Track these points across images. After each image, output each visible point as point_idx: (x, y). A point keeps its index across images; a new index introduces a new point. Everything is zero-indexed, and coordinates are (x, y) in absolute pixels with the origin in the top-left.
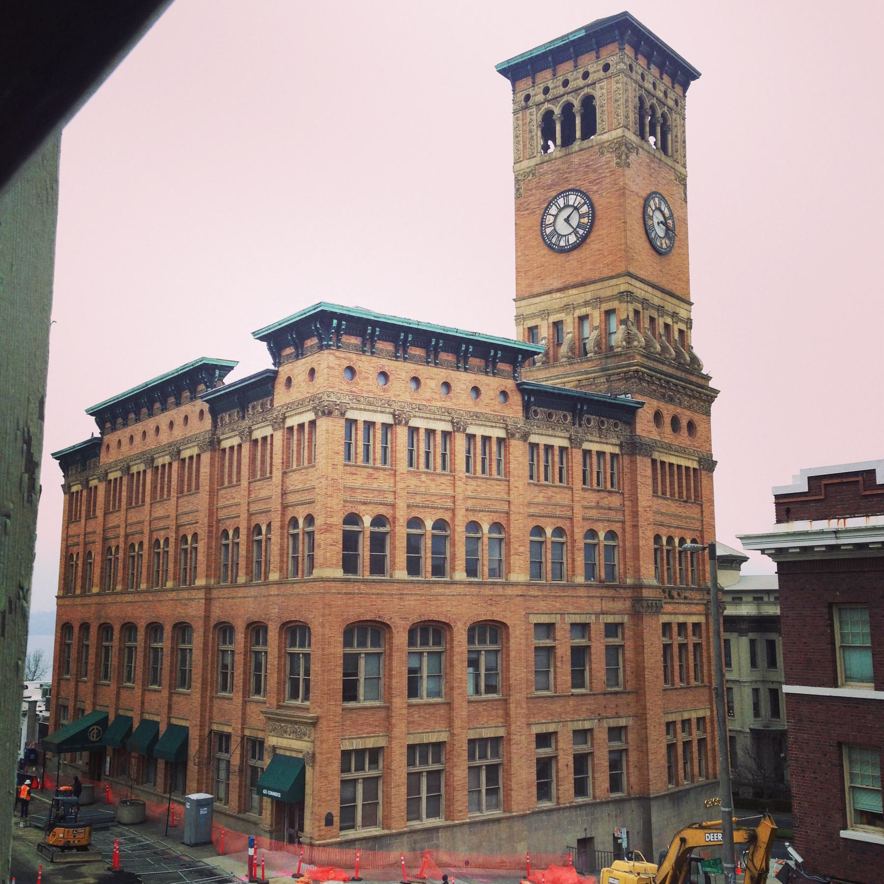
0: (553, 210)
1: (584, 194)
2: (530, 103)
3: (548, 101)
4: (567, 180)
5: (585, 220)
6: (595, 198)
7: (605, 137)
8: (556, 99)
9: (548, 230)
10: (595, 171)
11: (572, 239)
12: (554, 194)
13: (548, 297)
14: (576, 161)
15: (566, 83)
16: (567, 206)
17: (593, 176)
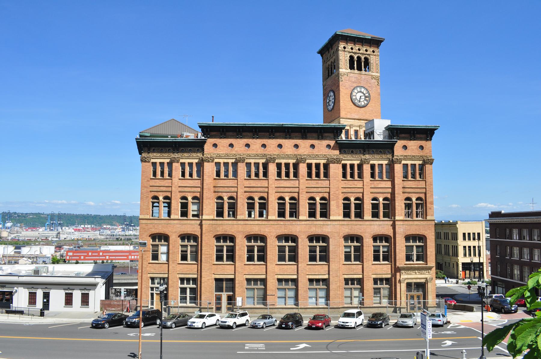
0: (356, 91)
1: (367, 90)
2: (346, 50)
3: (353, 53)
4: (360, 83)
5: (367, 99)
6: (370, 92)
7: (374, 74)
8: (355, 53)
9: (354, 97)
10: (370, 83)
11: (363, 104)
12: (355, 85)
14: (363, 77)
15: (359, 50)
16: (361, 92)
17: (369, 85)
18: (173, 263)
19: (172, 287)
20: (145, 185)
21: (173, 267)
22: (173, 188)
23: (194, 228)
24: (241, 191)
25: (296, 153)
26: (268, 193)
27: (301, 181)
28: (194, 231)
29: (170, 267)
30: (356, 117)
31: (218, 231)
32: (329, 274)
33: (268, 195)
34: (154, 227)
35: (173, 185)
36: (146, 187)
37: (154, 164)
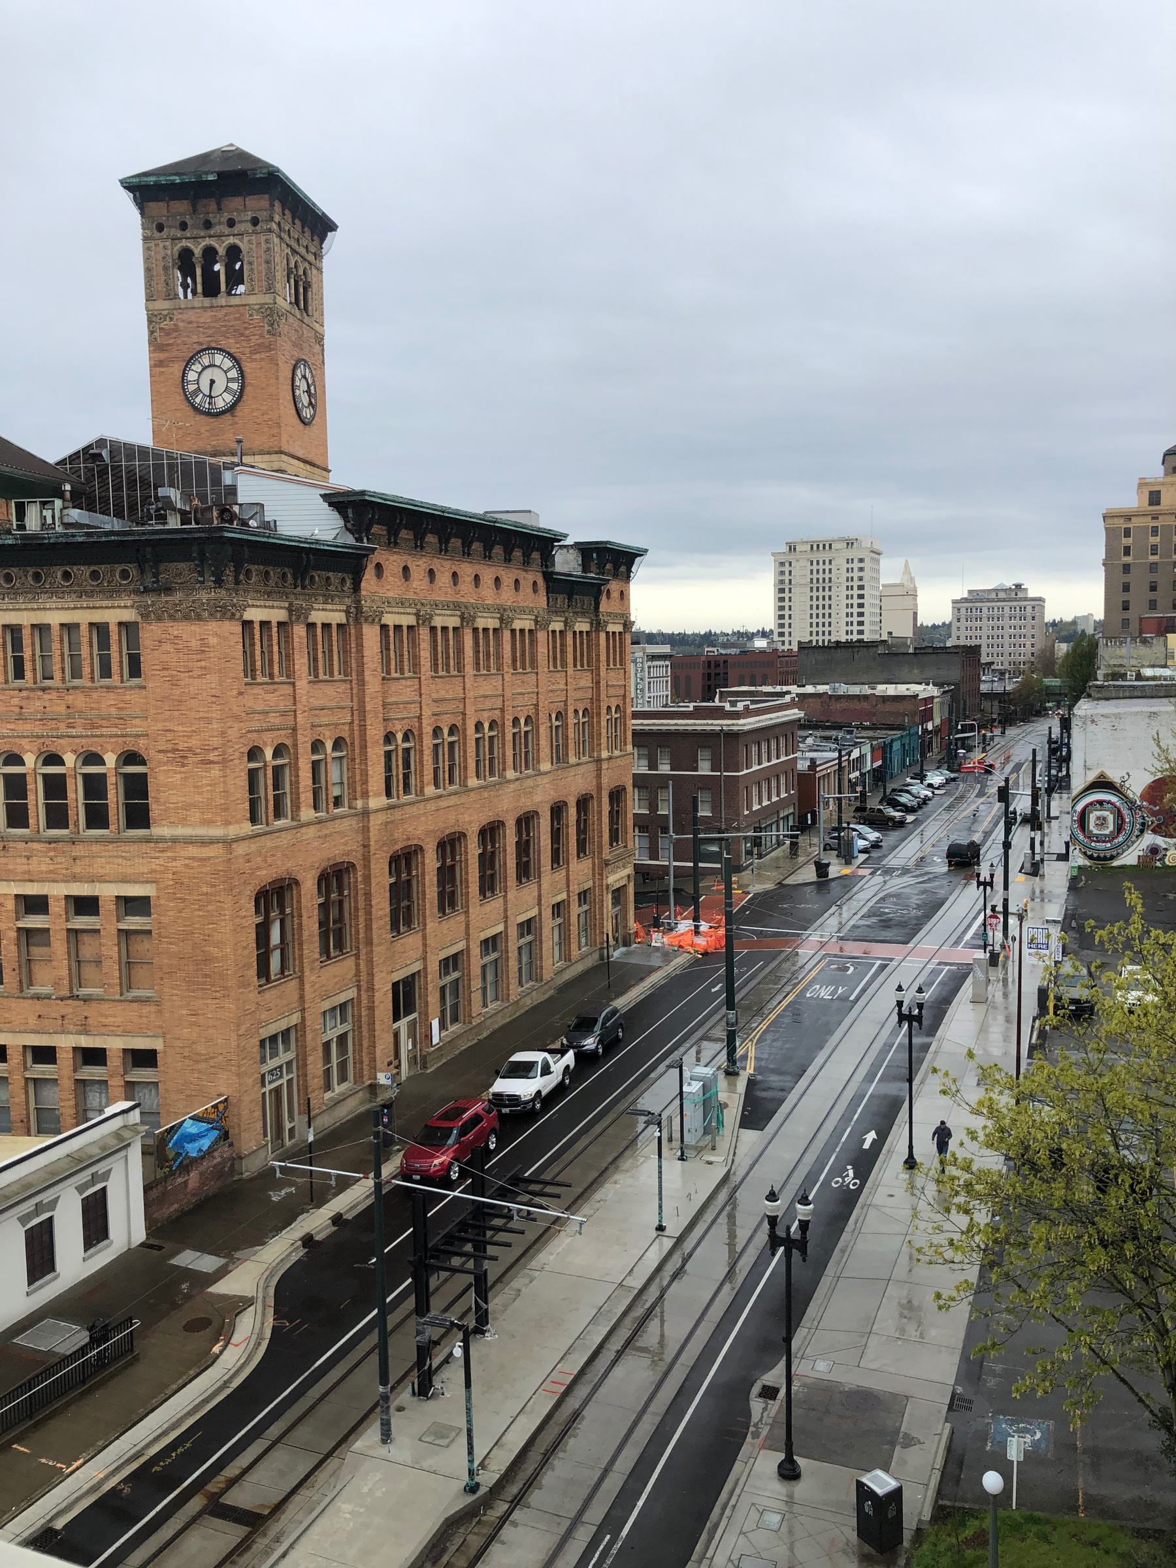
13: (302, 465)
18: (312, 969)
19: (314, 1049)
20: (237, 710)
21: (313, 984)
22: (300, 718)
23: (346, 844)
24: (427, 712)
25: (498, 601)
26: (464, 714)
27: (507, 677)
28: (348, 854)
29: (307, 986)
30: (300, 454)
31: (395, 842)
32: (539, 904)
33: (464, 720)
34: (265, 861)
35: (299, 706)
36: (237, 718)
37: (247, 624)
